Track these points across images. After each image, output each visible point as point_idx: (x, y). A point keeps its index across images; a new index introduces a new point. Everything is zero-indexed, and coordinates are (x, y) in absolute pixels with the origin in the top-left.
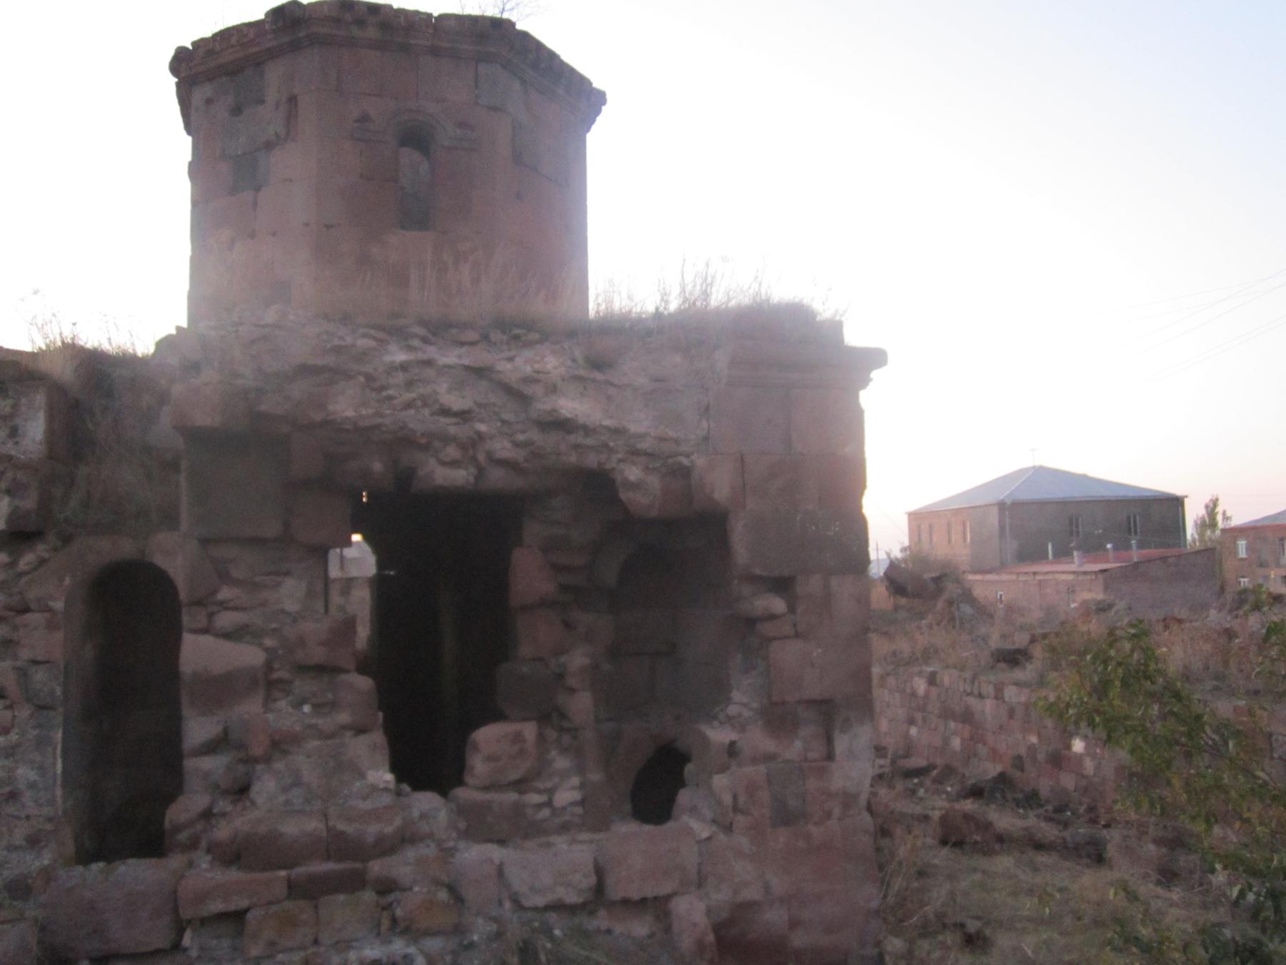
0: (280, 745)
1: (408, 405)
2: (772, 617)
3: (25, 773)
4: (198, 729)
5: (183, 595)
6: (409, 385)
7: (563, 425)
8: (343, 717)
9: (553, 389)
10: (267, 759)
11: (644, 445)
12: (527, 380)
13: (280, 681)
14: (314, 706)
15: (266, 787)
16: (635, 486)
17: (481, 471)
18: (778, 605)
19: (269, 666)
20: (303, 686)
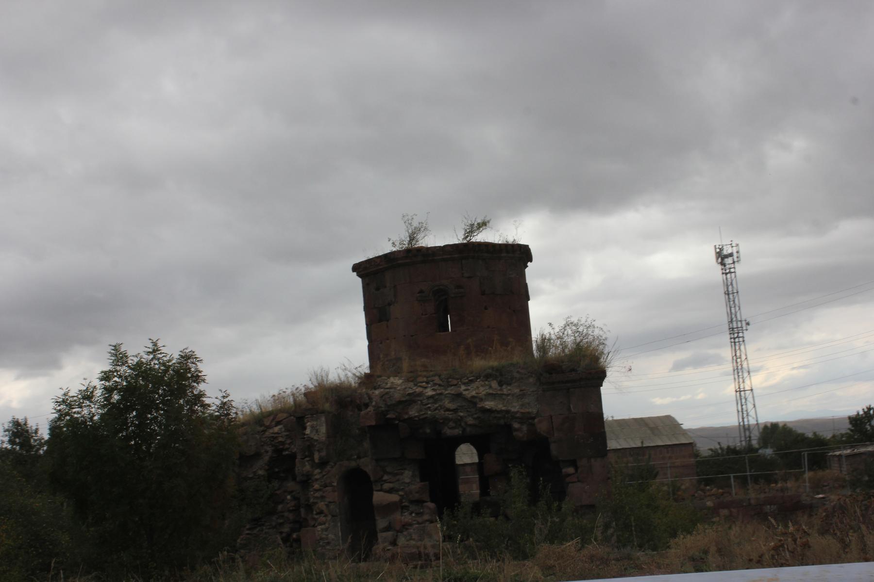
0: (405, 526)
1: (436, 409)
2: (569, 475)
3: (331, 536)
4: (381, 523)
5: (372, 479)
6: (436, 401)
7: (490, 411)
8: (426, 517)
9: (481, 400)
10: (401, 532)
11: (518, 415)
12: (473, 397)
13: (406, 506)
14: (417, 514)
15: (402, 541)
16: (517, 430)
17: (464, 430)
18: (571, 470)
19: (401, 501)
20: (413, 508)
